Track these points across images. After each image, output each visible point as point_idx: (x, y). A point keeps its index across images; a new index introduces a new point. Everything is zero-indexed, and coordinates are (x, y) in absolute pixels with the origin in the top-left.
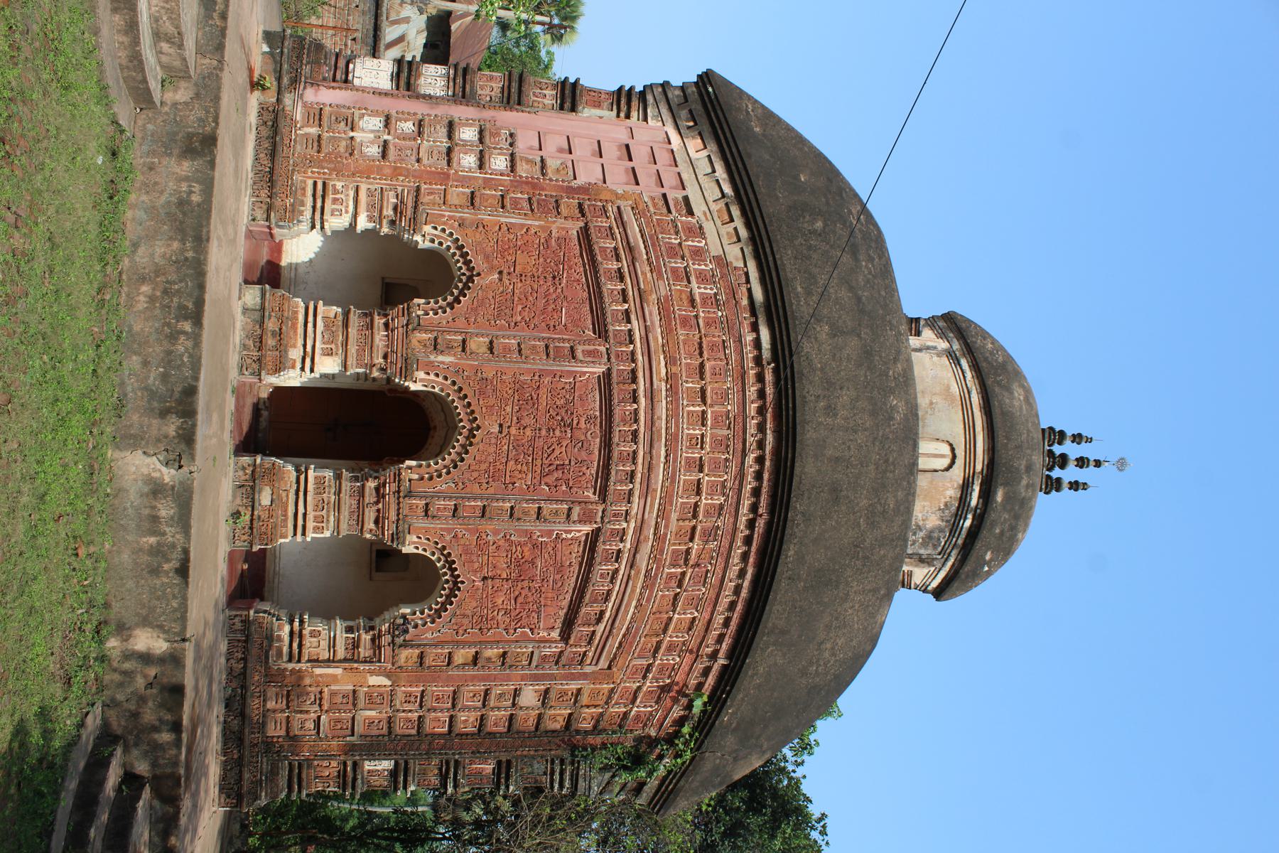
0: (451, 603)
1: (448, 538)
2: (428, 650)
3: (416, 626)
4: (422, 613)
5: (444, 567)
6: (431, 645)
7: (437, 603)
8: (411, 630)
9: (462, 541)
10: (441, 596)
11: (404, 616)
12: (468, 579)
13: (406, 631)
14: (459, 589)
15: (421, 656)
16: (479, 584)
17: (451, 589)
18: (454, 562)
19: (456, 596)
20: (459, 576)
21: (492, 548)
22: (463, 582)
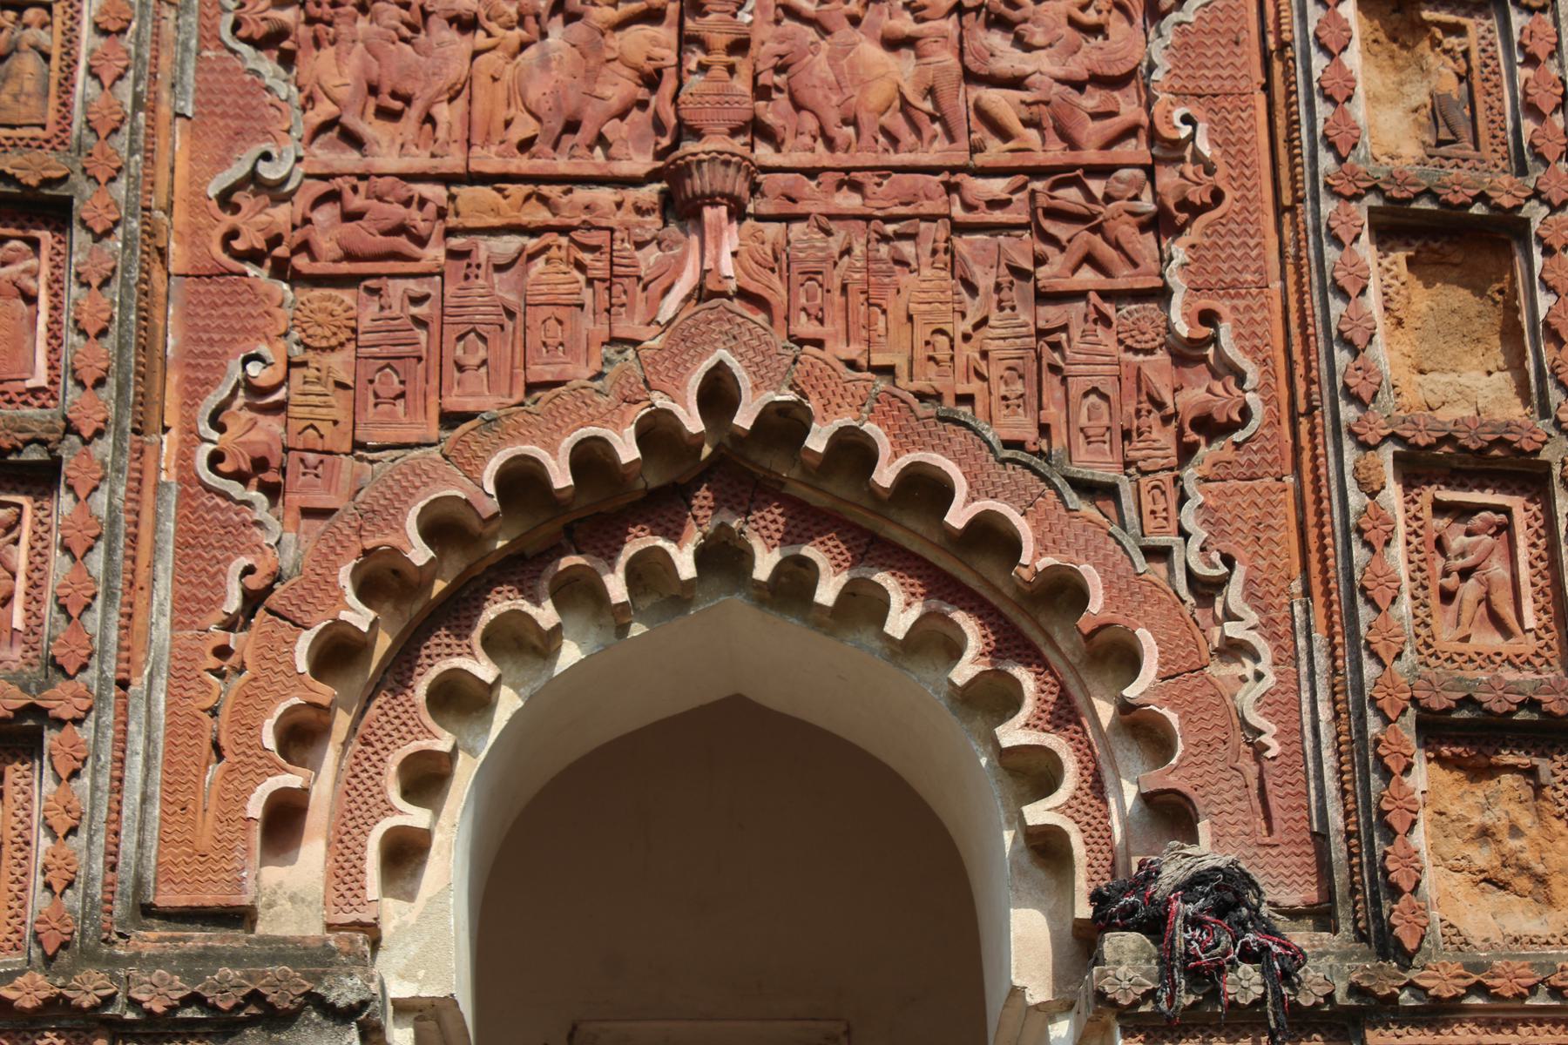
0: (926, 490)
1: (282, 541)
2: (1397, 675)
3: (1171, 814)
4: (1035, 774)
5: (579, 594)
6: (1351, 643)
7: (936, 642)
8: (1208, 850)
9: (320, 409)
10: (862, 605)
11: (1081, 945)
12: (684, 339)
13: (1227, 893)
14: (784, 424)
15: (1470, 736)
16: (727, 248)
17: (806, 521)
18: (521, 481)
19: (854, 451)
20: (657, 433)
21: (392, 148)
22: (718, 394)
